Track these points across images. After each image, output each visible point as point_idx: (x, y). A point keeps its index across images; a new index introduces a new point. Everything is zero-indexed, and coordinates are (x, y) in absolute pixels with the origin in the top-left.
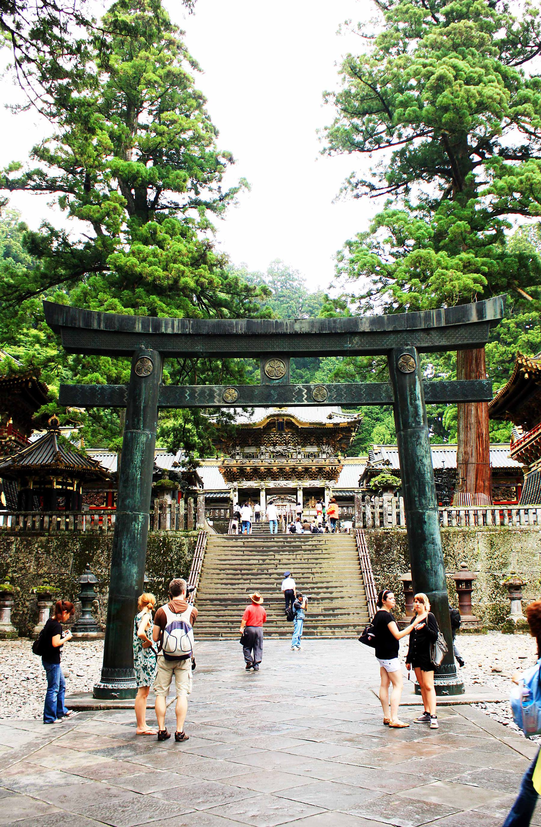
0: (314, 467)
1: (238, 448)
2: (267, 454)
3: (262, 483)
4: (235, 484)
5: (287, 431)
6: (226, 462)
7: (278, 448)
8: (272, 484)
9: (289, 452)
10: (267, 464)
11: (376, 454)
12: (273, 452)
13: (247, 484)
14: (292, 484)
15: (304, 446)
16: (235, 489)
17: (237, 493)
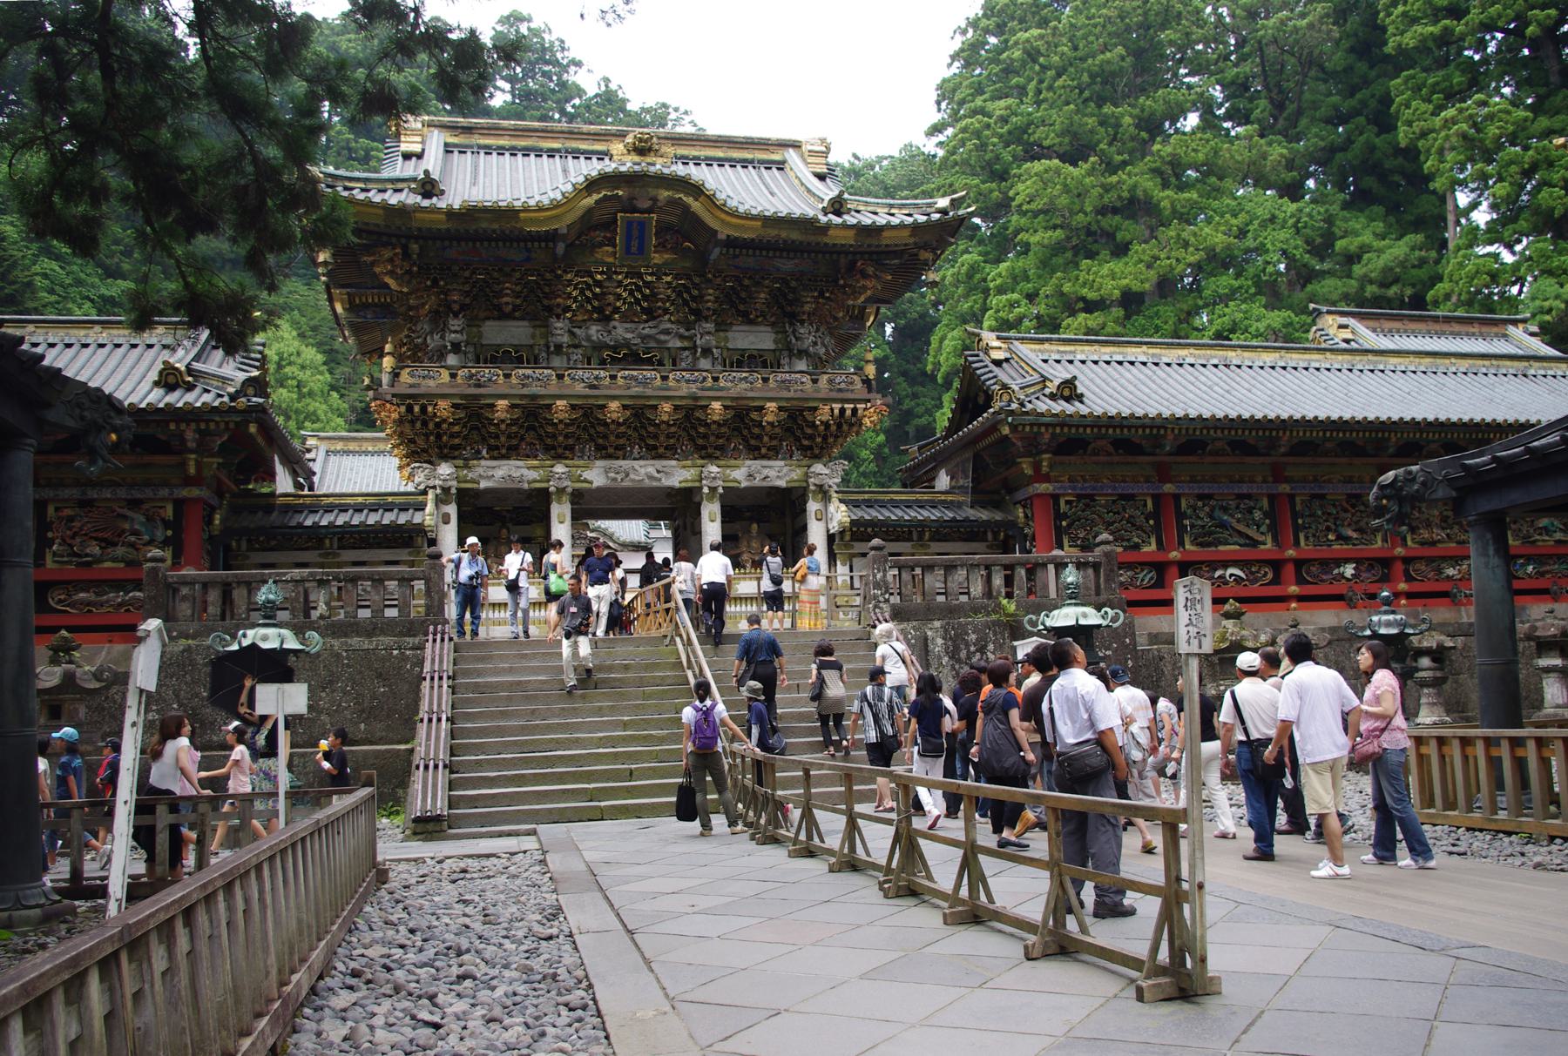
0: (772, 406)
1: (455, 323)
2: (577, 355)
3: (560, 469)
4: (445, 469)
5: (657, 259)
6: (405, 376)
7: (622, 331)
8: (596, 475)
9: (662, 347)
10: (580, 388)
11: (998, 363)
12: (599, 347)
13: (496, 474)
14: (677, 474)
15: (722, 326)
16: (446, 490)
17: (452, 509)
